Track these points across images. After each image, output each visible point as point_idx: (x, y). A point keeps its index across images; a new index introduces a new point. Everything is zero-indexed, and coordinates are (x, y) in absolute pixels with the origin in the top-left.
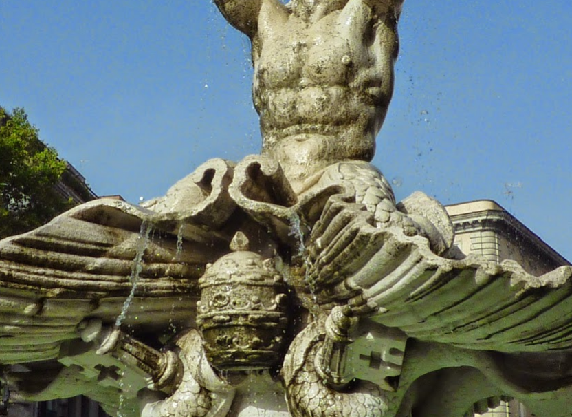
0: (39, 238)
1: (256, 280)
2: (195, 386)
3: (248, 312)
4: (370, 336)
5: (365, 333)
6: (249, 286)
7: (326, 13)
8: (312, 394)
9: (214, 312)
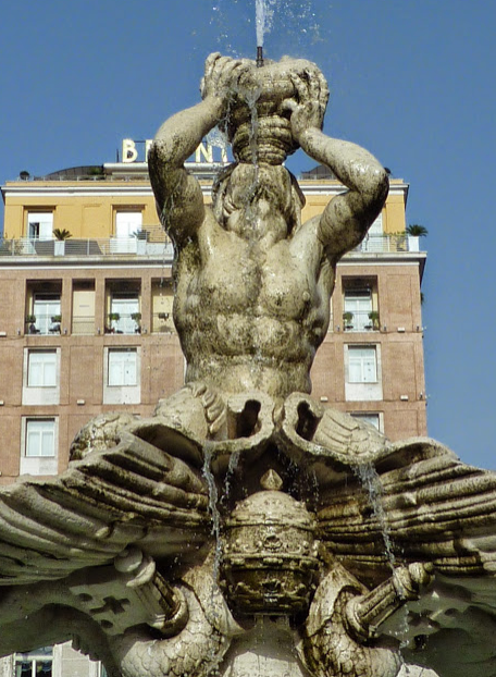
0: (128, 456)
1: (306, 524)
2: (206, 628)
3: (301, 557)
4: (435, 595)
5: (430, 591)
6: (300, 529)
7: (276, 241)
8: (342, 648)
9: (263, 553)
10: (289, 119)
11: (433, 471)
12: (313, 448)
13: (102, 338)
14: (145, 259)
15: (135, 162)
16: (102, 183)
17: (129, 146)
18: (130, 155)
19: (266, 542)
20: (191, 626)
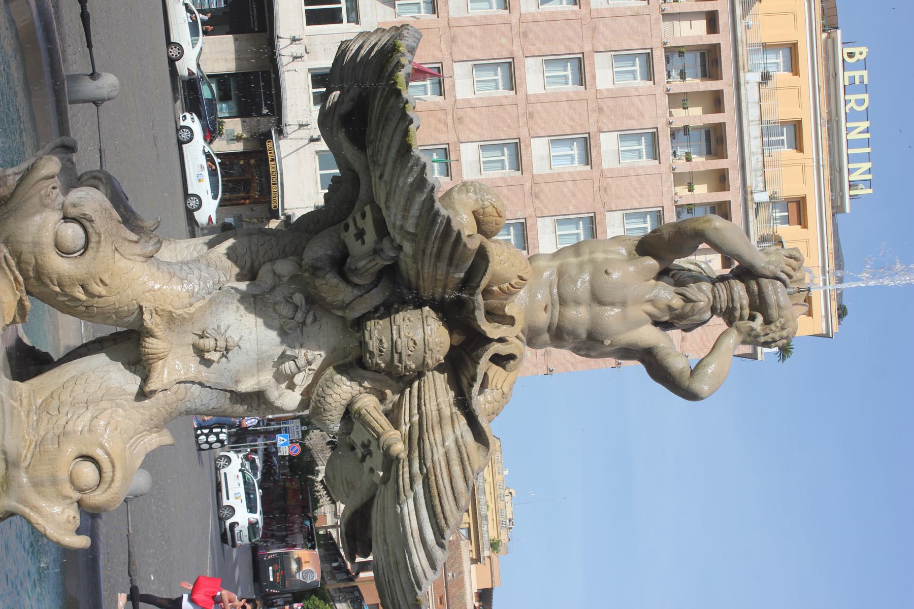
7: (650, 315)
10: (749, 319)
11: (468, 457)
12: (484, 361)
13: (660, 45)
14: (742, 81)
15: (844, 60)
16: (819, 29)
17: (861, 53)
18: (851, 55)
19: (412, 339)
20: (350, 289)
